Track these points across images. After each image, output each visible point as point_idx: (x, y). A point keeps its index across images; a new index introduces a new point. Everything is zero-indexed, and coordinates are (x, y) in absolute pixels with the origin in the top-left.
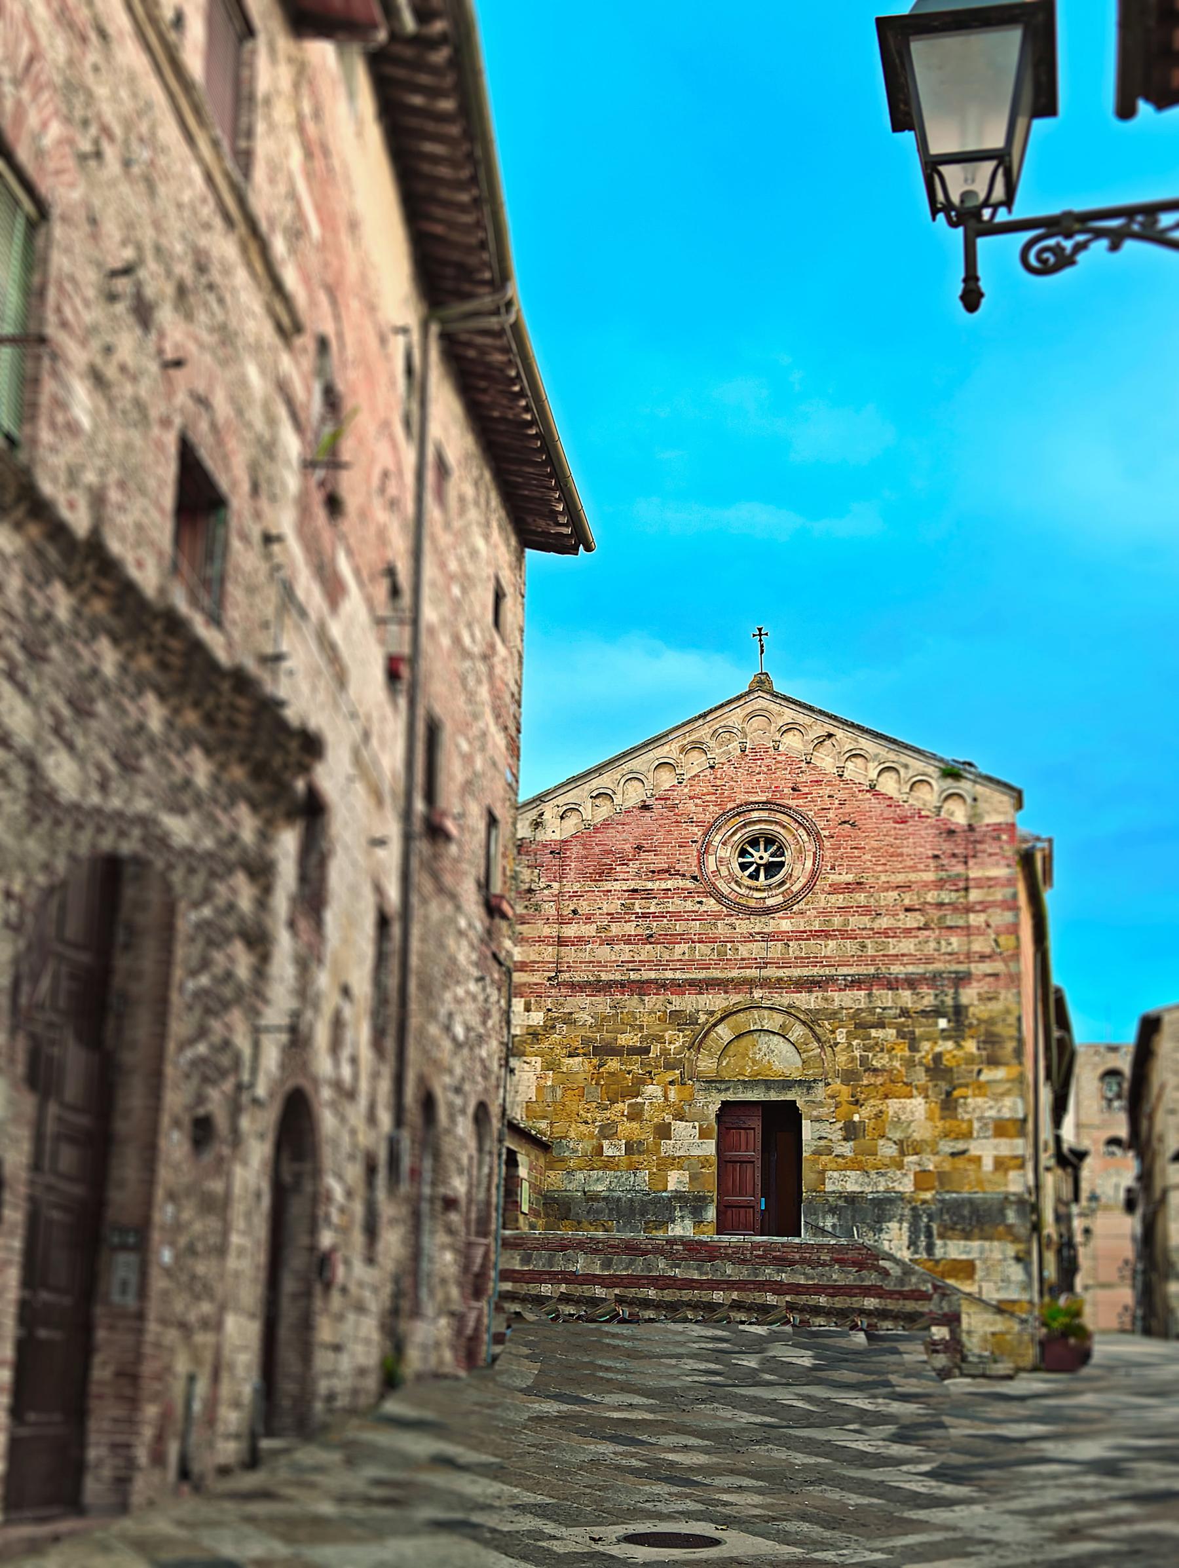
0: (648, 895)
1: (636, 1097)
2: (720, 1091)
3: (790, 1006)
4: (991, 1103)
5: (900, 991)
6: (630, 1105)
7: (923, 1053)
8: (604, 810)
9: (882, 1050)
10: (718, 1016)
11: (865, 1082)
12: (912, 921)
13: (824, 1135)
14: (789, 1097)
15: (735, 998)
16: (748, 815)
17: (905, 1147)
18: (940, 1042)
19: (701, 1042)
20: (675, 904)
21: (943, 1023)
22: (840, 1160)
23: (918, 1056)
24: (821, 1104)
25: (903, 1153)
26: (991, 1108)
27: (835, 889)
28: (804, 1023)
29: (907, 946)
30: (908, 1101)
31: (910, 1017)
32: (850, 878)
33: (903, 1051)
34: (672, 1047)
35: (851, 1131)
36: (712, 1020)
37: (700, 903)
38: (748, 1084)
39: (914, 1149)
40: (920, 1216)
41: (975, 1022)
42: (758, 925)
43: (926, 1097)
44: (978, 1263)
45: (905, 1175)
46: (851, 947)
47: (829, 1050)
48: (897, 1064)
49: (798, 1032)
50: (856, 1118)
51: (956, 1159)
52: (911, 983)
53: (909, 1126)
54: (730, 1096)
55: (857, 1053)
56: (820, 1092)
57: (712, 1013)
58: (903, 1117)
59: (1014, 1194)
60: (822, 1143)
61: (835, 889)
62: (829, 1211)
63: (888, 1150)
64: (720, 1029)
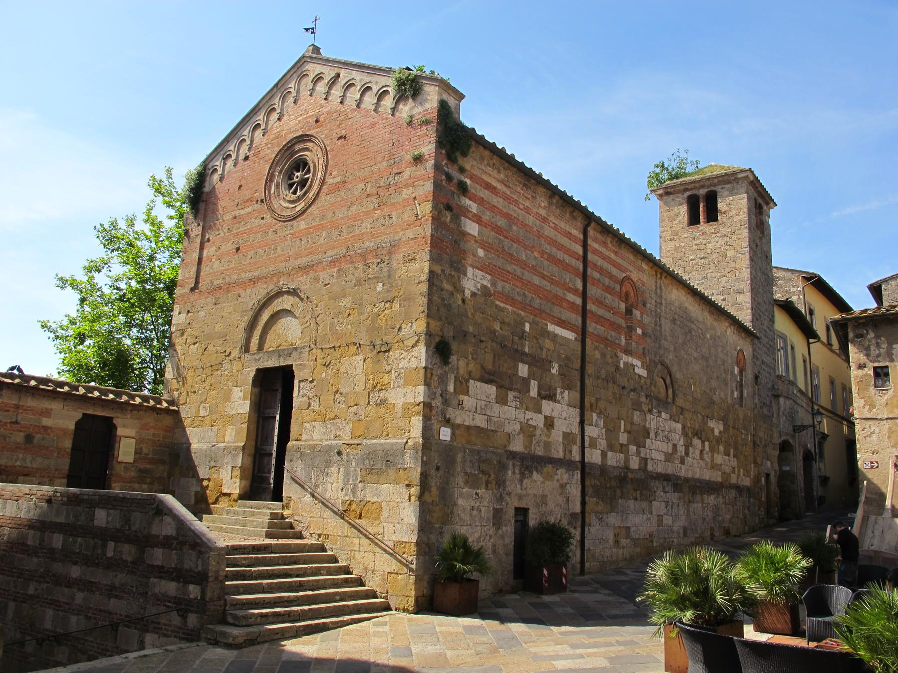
31: (361, 285)
37: (263, 218)
44: (384, 504)
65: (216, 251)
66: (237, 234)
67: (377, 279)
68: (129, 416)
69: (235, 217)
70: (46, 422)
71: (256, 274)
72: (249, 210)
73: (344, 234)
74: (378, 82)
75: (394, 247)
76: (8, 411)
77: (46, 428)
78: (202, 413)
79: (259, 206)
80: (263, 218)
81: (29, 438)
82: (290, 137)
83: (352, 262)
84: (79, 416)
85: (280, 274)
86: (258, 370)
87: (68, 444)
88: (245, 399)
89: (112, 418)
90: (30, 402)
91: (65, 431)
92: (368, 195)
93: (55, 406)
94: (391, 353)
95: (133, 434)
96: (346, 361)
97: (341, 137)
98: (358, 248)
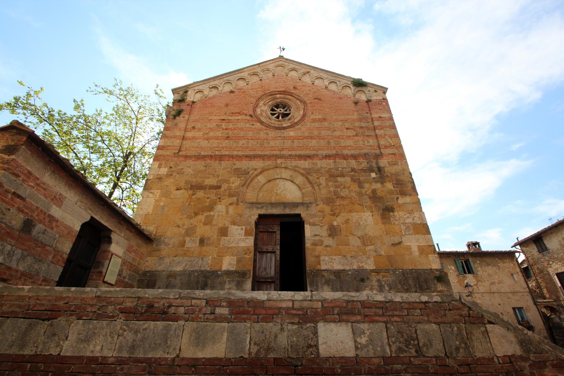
0: (229, 121)
1: (210, 211)
2: (258, 208)
3: (296, 167)
4: (408, 215)
5: (350, 160)
6: (207, 216)
7: (366, 189)
8: (214, 92)
9: (345, 188)
10: (259, 171)
11: (338, 203)
12: (350, 133)
13: (318, 233)
14: (297, 211)
15: (268, 163)
16: (275, 96)
17: (366, 240)
18: (374, 184)
19: (249, 184)
20: (240, 125)
21: (373, 175)
22: (328, 249)
23: (364, 191)
24: (314, 216)
25: (364, 244)
26: (408, 217)
27: (314, 121)
28: (302, 174)
29: (349, 142)
30: (363, 214)
31: (356, 172)
32: (320, 117)
33: (355, 187)
34: (234, 185)
35: (333, 231)
36: (256, 173)
37: (253, 125)
38: (273, 205)
39: (371, 242)
40: (384, 286)
41: (390, 175)
42: (279, 133)
43: (372, 212)
45: (368, 258)
46: (323, 143)
47: (316, 188)
48: (353, 194)
49: (300, 179)
50: (335, 223)
51: (396, 247)
52: (355, 157)
53: (365, 228)
54: (263, 212)
55: (332, 189)
56: (314, 209)
57: (256, 170)
58: (361, 223)
59: (437, 270)
60: (317, 238)
61: (314, 121)
62: (325, 283)
63: (355, 242)
64: (259, 178)
65: (203, 134)
66: (226, 129)
67: (371, 170)
68: (123, 235)
69: (224, 120)
70: (55, 211)
71: (252, 153)
72: (239, 118)
73: (332, 144)
74: (344, 82)
75: (378, 156)
76: (17, 176)
77: (52, 219)
78: (188, 245)
79: (248, 118)
80: (253, 125)
81: (28, 225)
82: (272, 90)
83: (345, 159)
84: (88, 218)
85: (277, 157)
86: (259, 215)
87: (66, 247)
88: (247, 233)
89: (111, 231)
90: (48, 179)
91: (70, 229)
92: (347, 129)
93: (71, 196)
94: (396, 213)
95: (121, 255)
96: (355, 217)
97: (316, 99)
98: (345, 152)
